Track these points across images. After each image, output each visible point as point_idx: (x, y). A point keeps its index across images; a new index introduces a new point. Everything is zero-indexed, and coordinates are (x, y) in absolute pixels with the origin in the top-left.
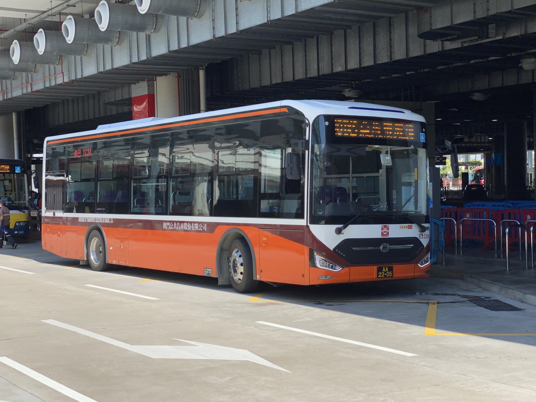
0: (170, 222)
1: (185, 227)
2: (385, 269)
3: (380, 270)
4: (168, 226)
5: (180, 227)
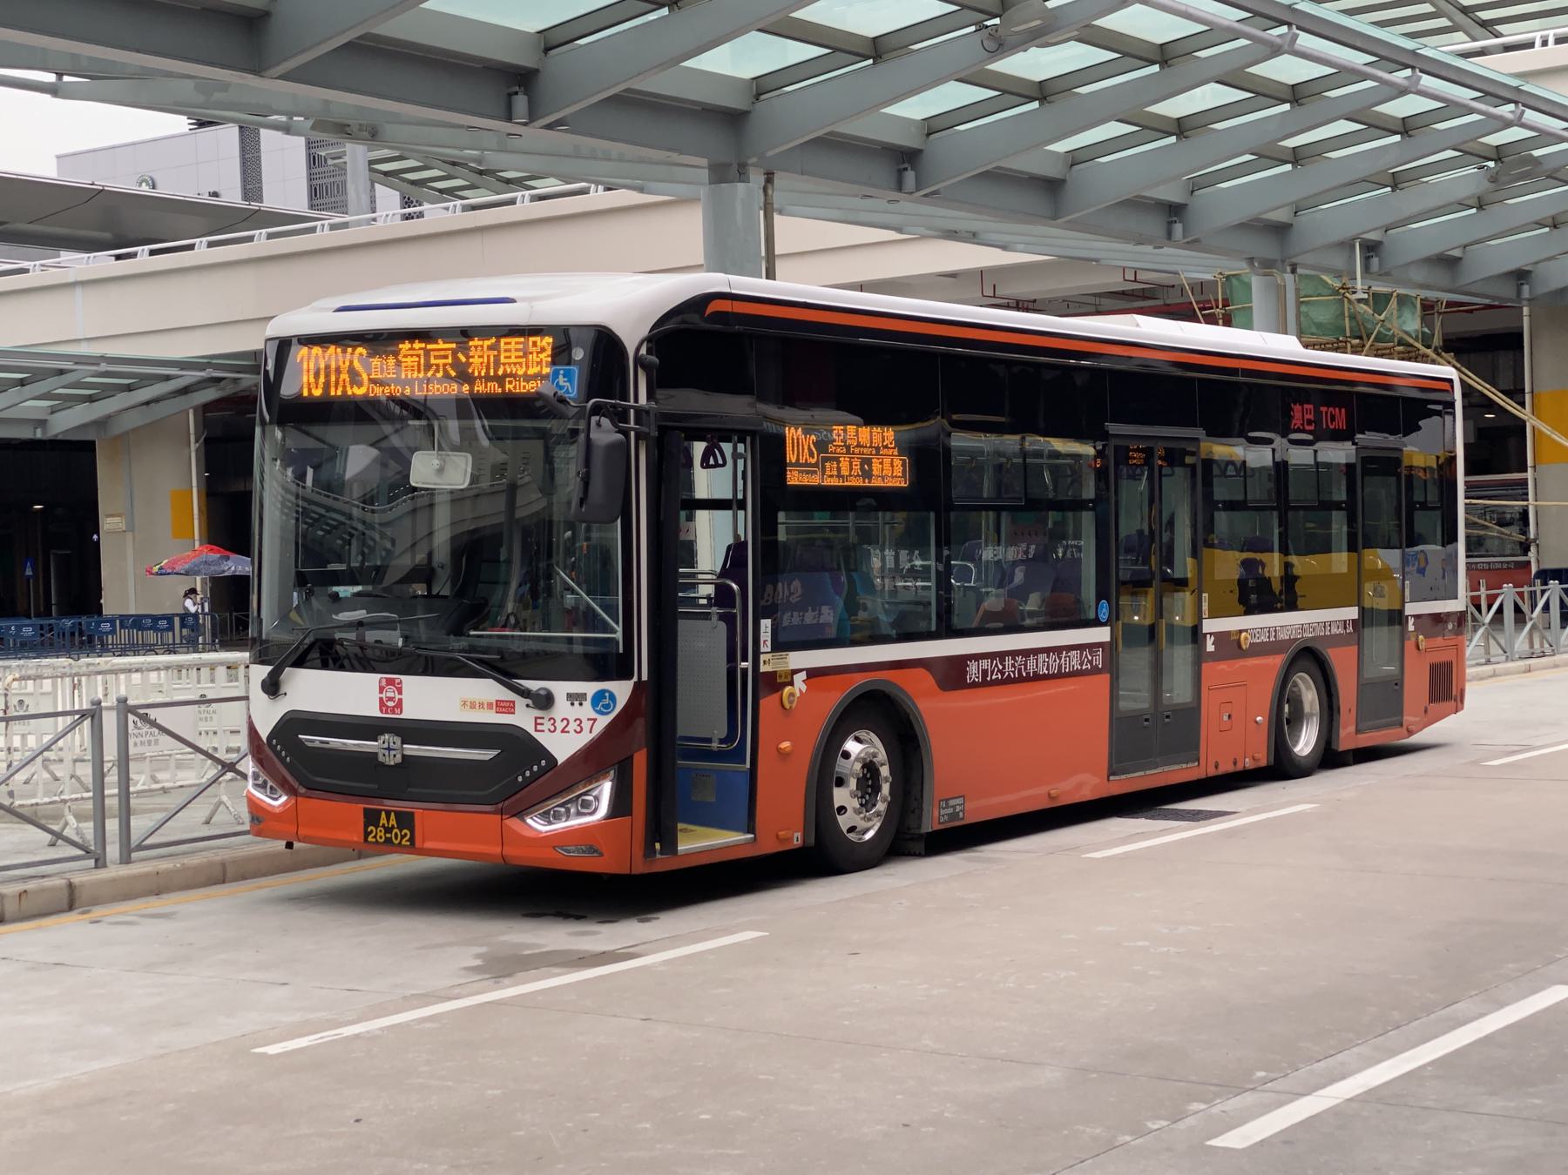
1: (1040, 665)
2: (388, 819)
3: (371, 818)
5: (1026, 669)
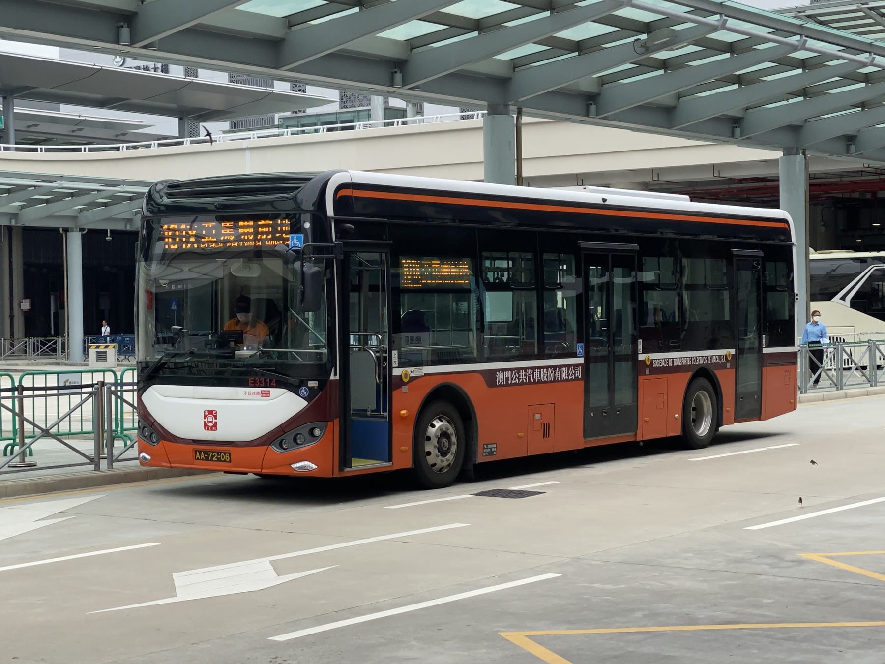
0: (512, 370)
1: (542, 376)
4: (507, 379)
